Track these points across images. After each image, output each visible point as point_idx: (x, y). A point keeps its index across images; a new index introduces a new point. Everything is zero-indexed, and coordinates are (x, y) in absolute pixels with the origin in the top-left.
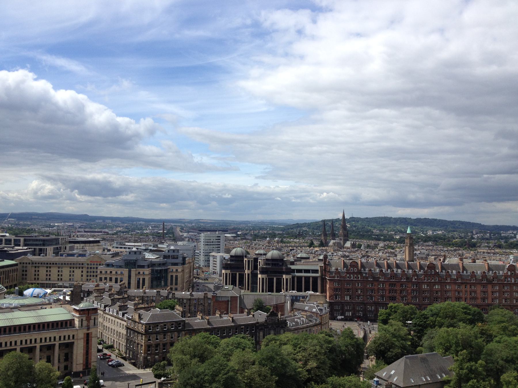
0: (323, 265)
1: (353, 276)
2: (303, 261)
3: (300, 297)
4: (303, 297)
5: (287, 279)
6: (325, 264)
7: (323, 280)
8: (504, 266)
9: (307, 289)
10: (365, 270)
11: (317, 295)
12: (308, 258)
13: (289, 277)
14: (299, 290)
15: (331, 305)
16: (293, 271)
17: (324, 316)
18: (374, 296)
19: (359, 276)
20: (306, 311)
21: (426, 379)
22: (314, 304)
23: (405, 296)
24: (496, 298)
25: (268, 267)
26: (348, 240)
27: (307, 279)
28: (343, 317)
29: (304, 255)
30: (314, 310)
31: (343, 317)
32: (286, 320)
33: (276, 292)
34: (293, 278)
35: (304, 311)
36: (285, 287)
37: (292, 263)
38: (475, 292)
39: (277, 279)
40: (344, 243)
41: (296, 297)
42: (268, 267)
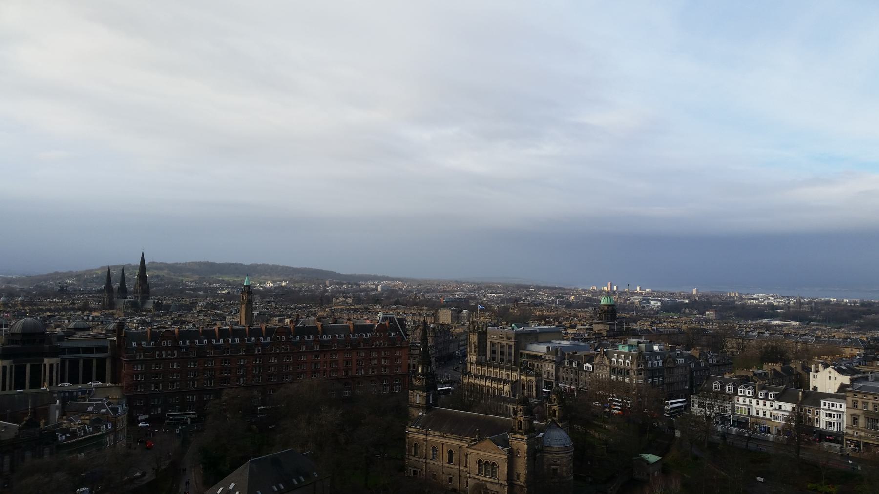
0: (115, 339)
1: (166, 353)
2: (79, 334)
3: (77, 392)
4: (84, 392)
5: (51, 366)
6: (119, 336)
7: (115, 361)
8: (372, 326)
9: (87, 379)
10: (184, 343)
11: (109, 387)
12: (88, 329)
13: (55, 361)
14: (74, 380)
15: (130, 401)
16: (63, 351)
17: (119, 418)
18: (197, 380)
19: (176, 352)
20: (90, 412)
21: (278, 487)
22: (102, 400)
23: (243, 376)
24: (361, 368)
25: (15, 346)
26: (149, 299)
27: (88, 363)
28: (147, 417)
29: (81, 324)
30: (104, 410)
31: (147, 417)
32: (55, 432)
33: (31, 387)
34: (63, 362)
35: (85, 412)
36: (47, 378)
37: (60, 338)
38: (336, 362)
39: (32, 366)
40: (143, 303)
41: (71, 393)
42: (15, 346)
